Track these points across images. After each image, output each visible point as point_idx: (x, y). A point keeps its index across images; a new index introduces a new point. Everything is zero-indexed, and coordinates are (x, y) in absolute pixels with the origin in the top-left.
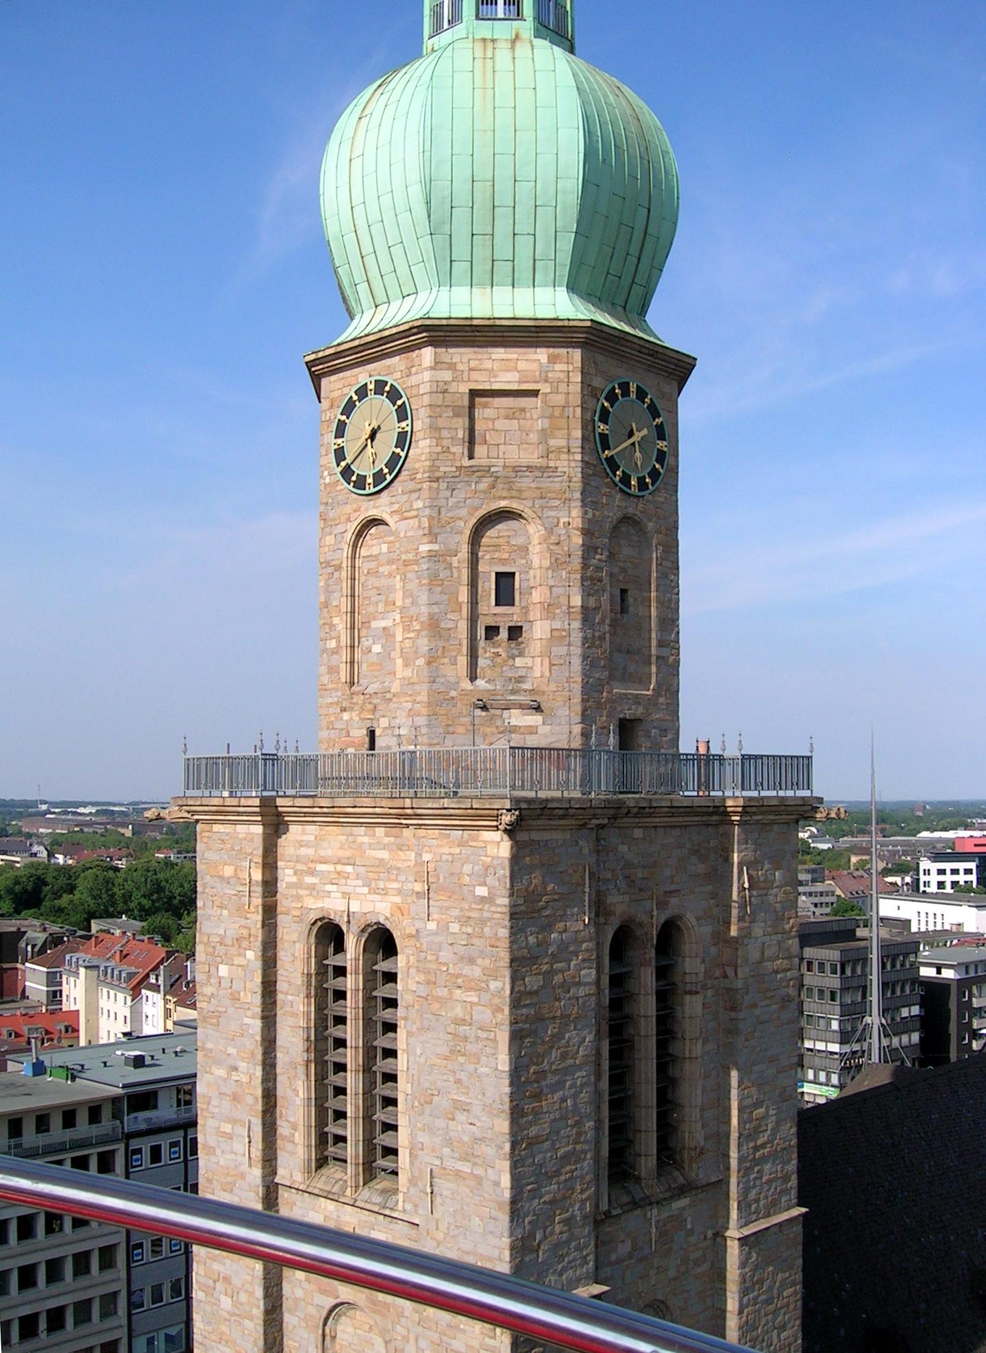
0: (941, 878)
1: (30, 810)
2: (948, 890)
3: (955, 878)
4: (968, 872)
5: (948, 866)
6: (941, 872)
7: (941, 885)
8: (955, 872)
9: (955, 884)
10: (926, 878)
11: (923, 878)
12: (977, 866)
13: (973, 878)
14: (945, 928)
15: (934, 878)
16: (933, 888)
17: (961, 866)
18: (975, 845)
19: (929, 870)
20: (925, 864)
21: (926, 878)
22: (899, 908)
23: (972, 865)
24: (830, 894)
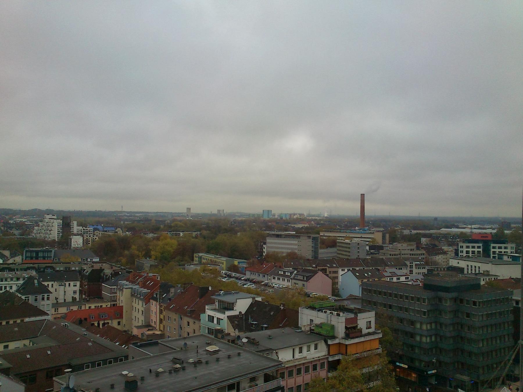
0: (468, 249)
1: (130, 217)
2: (470, 255)
3: (473, 250)
4: (479, 247)
5: (471, 245)
6: (468, 247)
7: (467, 252)
8: (473, 247)
9: (473, 252)
10: (462, 249)
11: (460, 249)
12: (482, 245)
13: (481, 250)
14: (480, 272)
15: (465, 250)
16: (465, 254)
17: (476, 245)
18: (482, 237)
19: (463, 246)
20: (461, 244)
21: (462, 249)
22: (458, 263)
23: (481, 245)
24: (396, 255)
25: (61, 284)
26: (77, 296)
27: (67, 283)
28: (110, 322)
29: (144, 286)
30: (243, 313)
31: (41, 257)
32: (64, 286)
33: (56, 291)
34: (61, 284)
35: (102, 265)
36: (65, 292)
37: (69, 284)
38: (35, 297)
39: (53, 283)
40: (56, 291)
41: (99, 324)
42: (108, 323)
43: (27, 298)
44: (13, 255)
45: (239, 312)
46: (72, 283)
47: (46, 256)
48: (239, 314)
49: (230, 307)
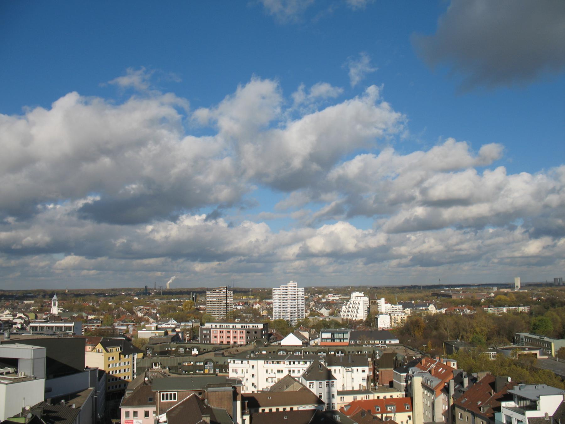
25: (348, 370)
26: (365, 384)
27: (355, 368)
28: (392, 415)
29: (437, 375)
30: (551, 414)
31: (337, 339)
32: (351, 372)
33: (343, 378)
34: (349, 369)
35: (397, 348)
36: (353, 378)
37: (357, 370)
38: (320, 383)
39: (340, 368)
40: (343, 378)
41: (382, 417)
42: (391, 417)
43: (311, 384)
44: (313, 337)
45: (545, 413)
46: (360, 369)
47: (342, 337)
48: (544, 416)
49: (533, 406)
